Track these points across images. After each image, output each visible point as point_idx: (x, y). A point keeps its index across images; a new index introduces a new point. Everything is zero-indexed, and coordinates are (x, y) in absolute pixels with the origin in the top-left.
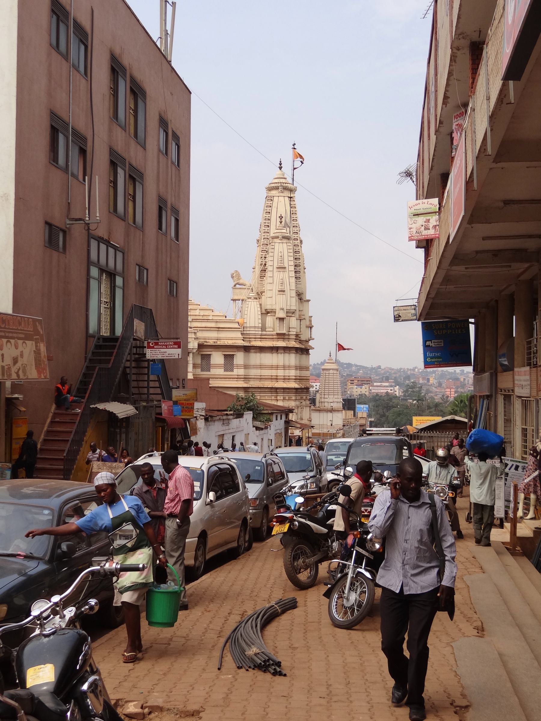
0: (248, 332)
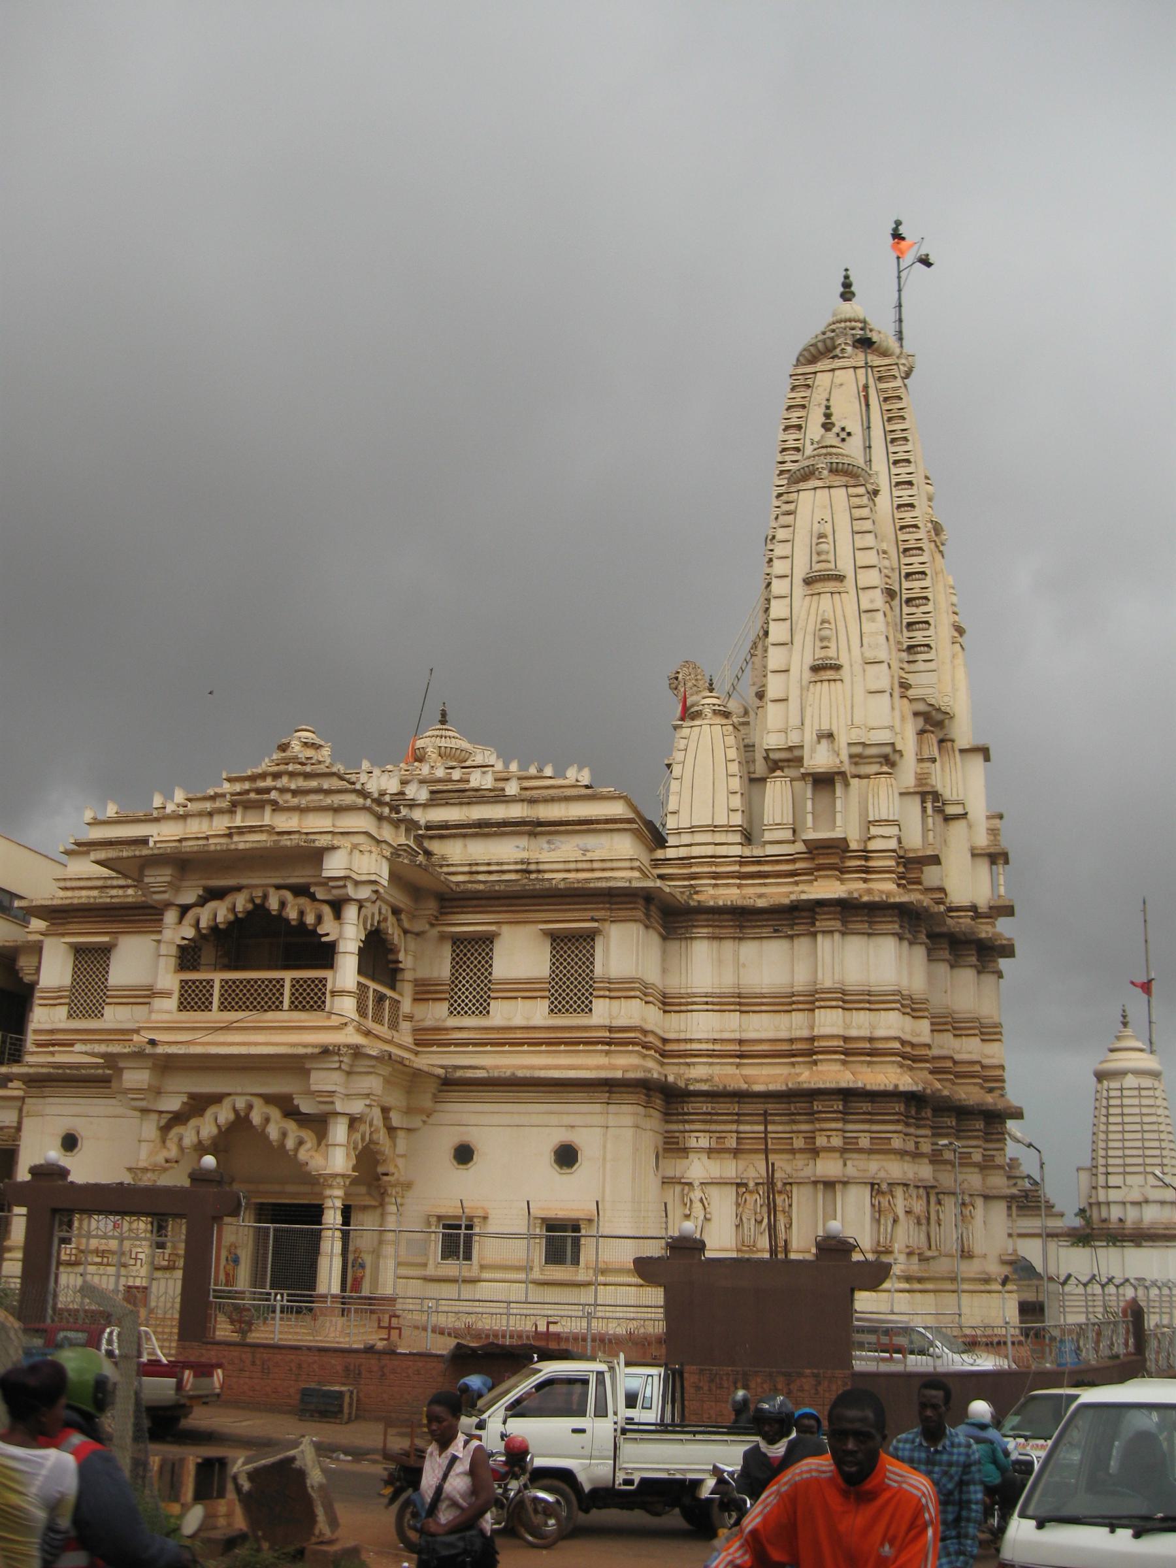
0: (683, 852)
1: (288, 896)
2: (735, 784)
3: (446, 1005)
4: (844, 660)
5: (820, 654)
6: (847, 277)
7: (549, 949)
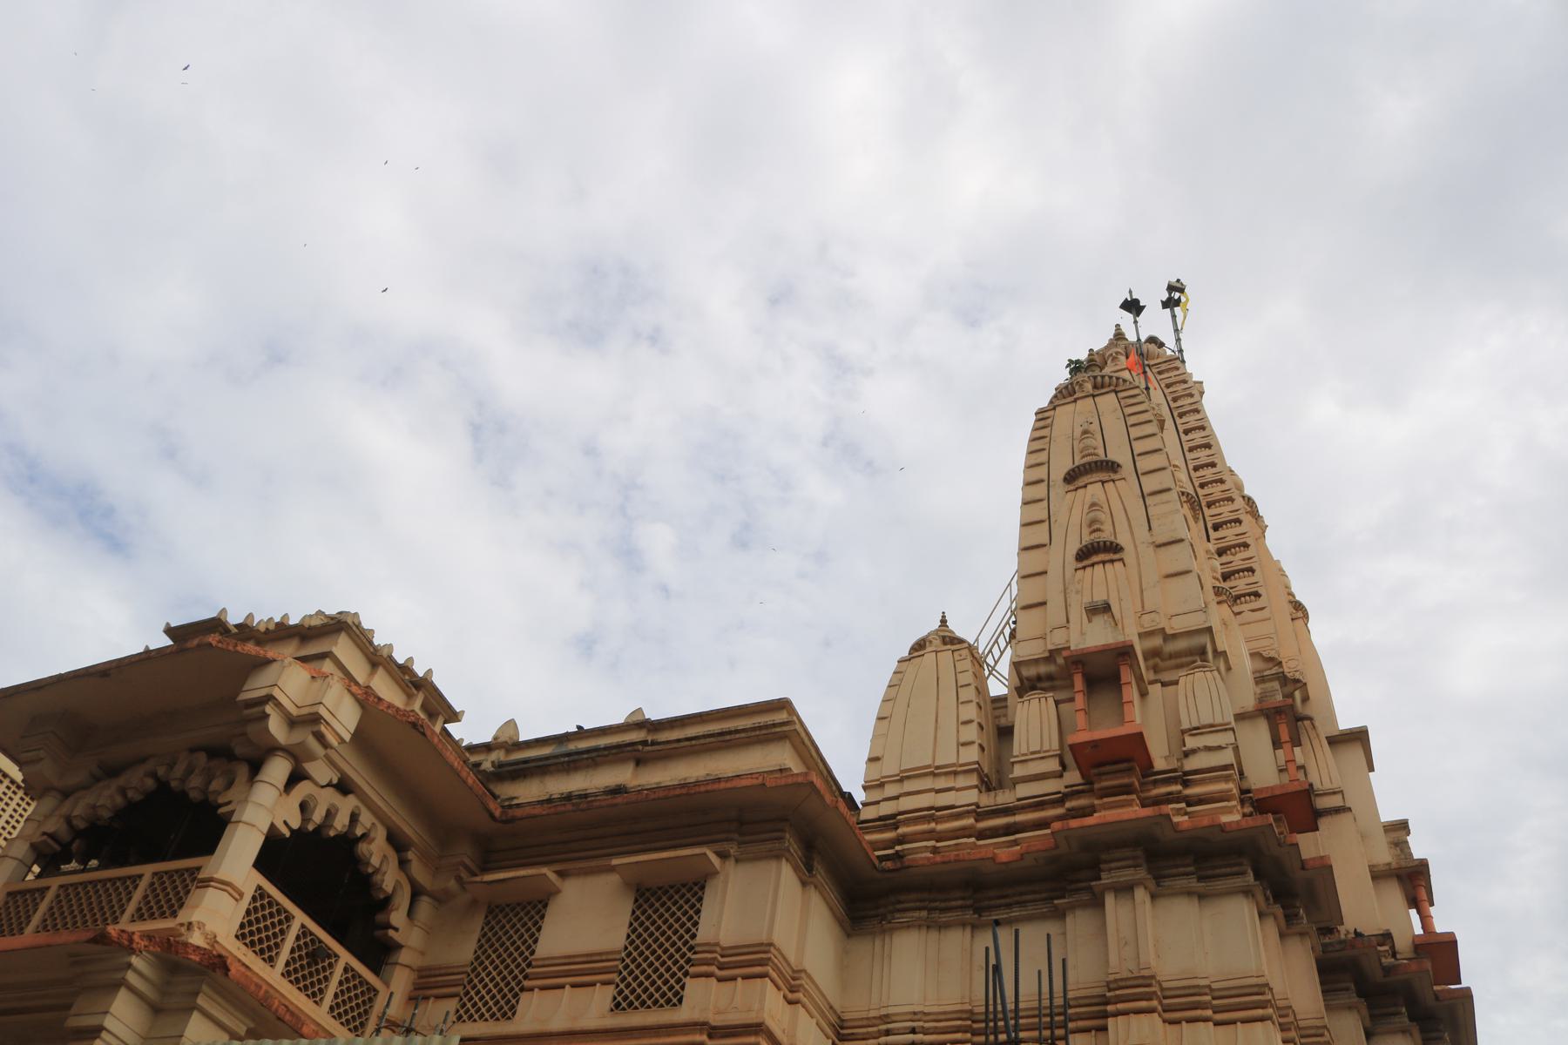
4: (1123, 539)
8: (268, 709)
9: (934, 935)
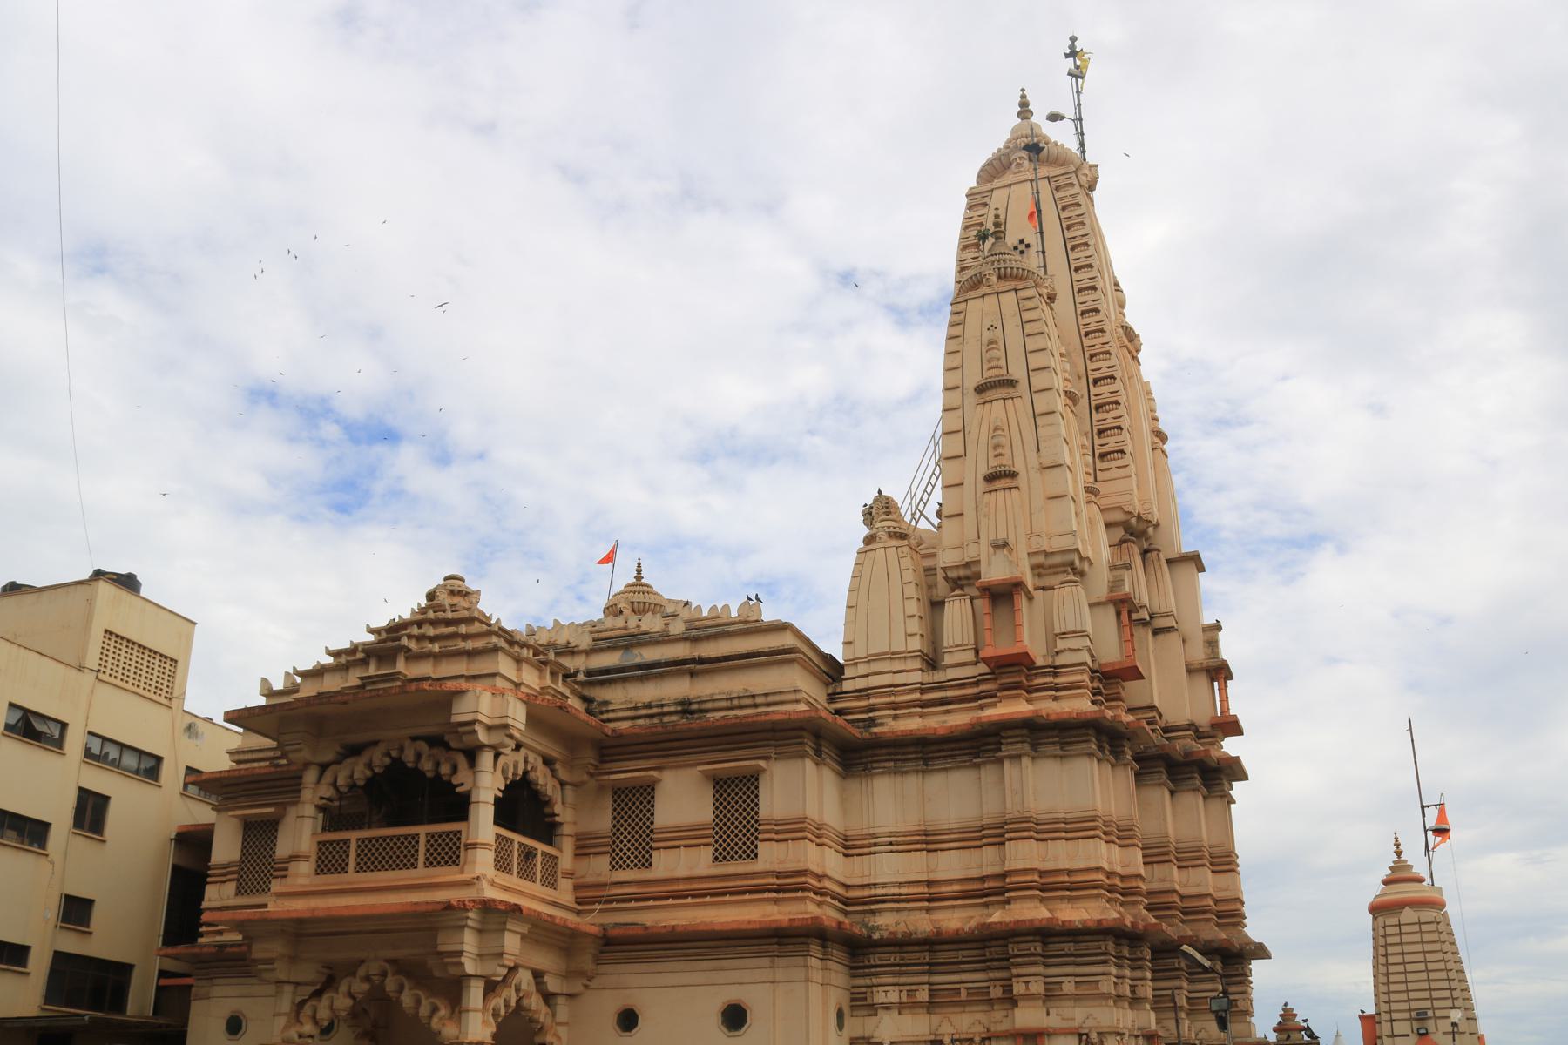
0: (860, 684)
1: (423, 746)
2: (913, 607)
3: (607, 858)
4: (1019, 466)
5: (994, 462)
6: (1023, 97)
7: (711, 791)
8: (477, 727)
9: (898, 779)
